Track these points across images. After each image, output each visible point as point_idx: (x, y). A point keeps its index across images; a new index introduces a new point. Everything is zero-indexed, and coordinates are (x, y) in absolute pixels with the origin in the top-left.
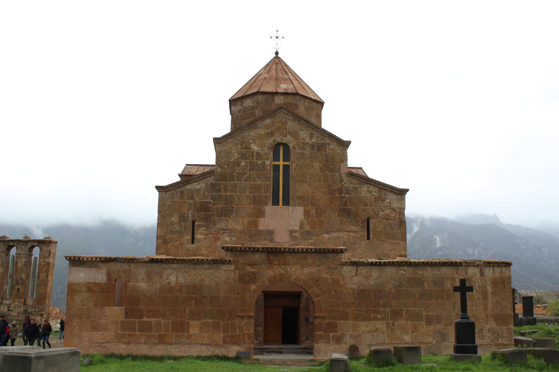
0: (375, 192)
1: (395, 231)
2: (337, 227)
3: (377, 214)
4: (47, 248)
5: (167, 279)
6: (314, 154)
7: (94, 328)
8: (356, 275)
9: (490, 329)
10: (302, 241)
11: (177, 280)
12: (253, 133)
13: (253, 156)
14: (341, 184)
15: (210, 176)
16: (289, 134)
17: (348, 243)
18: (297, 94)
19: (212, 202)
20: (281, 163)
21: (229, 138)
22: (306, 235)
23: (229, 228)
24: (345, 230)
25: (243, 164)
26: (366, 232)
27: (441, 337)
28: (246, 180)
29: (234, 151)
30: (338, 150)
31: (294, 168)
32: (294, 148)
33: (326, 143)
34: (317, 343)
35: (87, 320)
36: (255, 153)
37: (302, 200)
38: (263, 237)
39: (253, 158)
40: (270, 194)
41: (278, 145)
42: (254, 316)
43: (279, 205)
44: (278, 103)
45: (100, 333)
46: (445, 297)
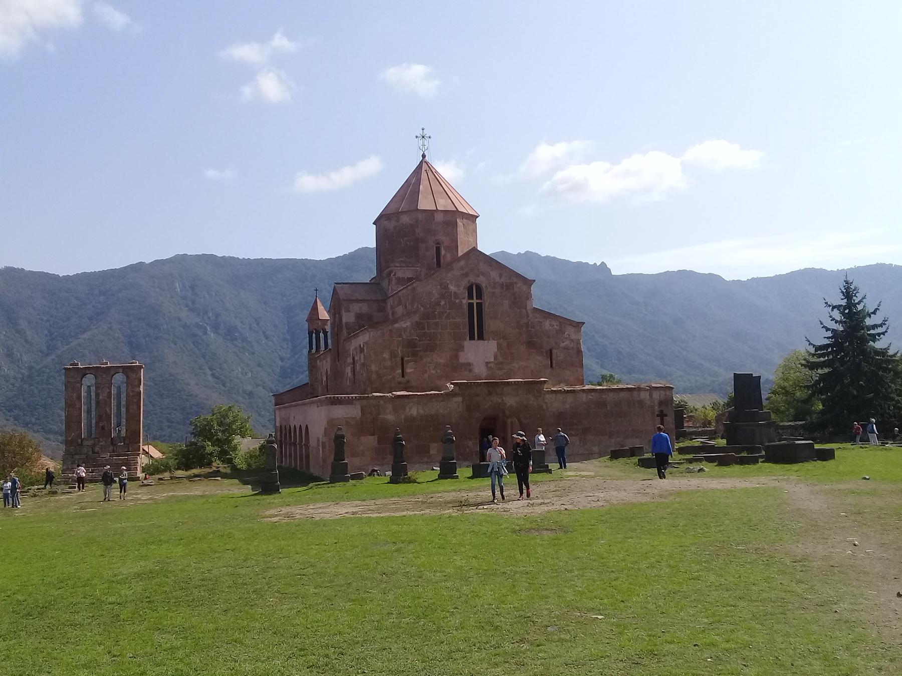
0: (557, 325)
12: (450, 275)
16: (483, 274)
19: (418, 339)
20: (475, 301)
25: (443, 303)
29: (434, 292)
30: (525, 288)
31: (487, 306)
32: (486, 287)
37: (496, 335)
38: (463, 368)
43: (474, 339)
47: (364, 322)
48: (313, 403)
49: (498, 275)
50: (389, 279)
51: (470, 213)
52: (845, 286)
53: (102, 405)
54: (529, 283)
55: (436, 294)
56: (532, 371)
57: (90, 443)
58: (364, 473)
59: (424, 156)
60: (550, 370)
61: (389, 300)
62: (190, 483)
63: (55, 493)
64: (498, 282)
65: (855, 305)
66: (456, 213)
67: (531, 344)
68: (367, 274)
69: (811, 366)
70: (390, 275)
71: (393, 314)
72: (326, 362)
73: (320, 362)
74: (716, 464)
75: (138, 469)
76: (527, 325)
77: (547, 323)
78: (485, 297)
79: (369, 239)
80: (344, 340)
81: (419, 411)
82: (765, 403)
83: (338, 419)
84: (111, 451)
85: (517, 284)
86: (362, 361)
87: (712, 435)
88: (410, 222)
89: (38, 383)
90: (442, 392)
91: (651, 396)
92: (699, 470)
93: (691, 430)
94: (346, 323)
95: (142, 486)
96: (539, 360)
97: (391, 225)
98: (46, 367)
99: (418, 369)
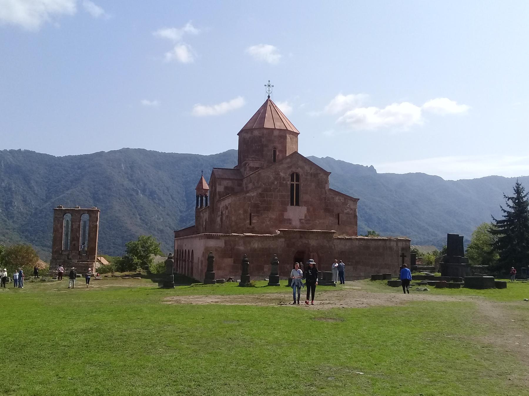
0: (343, 200)
5: (253, 245)
10: (306, 224)
12: (281, 167)
19: (260, 203)
20: (295, 183)
25: (276, 183)
29: (271, 176)
30: (324, 177)
32: (302, 175)
33: (318, 173)
37: (306, 203)
38: (286, 222)
39: (281, 181)
40: (290, 200)
43: (294, 205)
47: (229, 191)
48: (197, 237)
50: (245, 168)
51: (295, 131)
52: (516, 186)
53: (75, 231)
54: (327, 174)
55: (272, 178)
56: (327, 226)
57: (66, 253)
58: (224, 279)
59: (269, 97)
60: (338, 225)
61: (244, 180)
62: (123, 279)
63: (44, 281)
64: (309, 173)
65: (522, 198)
66: (287, 131)
67: (327, 210)
68: (232, 164)
69: (494, 232)
70: (246, 165)
71: (246, 188)
72: (206, 214)
73: (202, 214)
74: (434, 287)
75: (94, 270)
76: (325, 199)
77: (337, 198)
78: (301, 181)
79: (234, 145)
80: (217, 202)
82: (465, 253)
83: (211, 247)
84: (78, 258)
85: (320, 174)
86: (227, 214)
87: (433, 270)
88: (259, 135)
89: (40, 218)
90: (273, 235)
91: (397, 245)
92: (424, 290)
93: (420, 266)
94: (219, 192)
95: (95, 280)
96: (330, 220)
97: (247, 136)
98: (45, 208)
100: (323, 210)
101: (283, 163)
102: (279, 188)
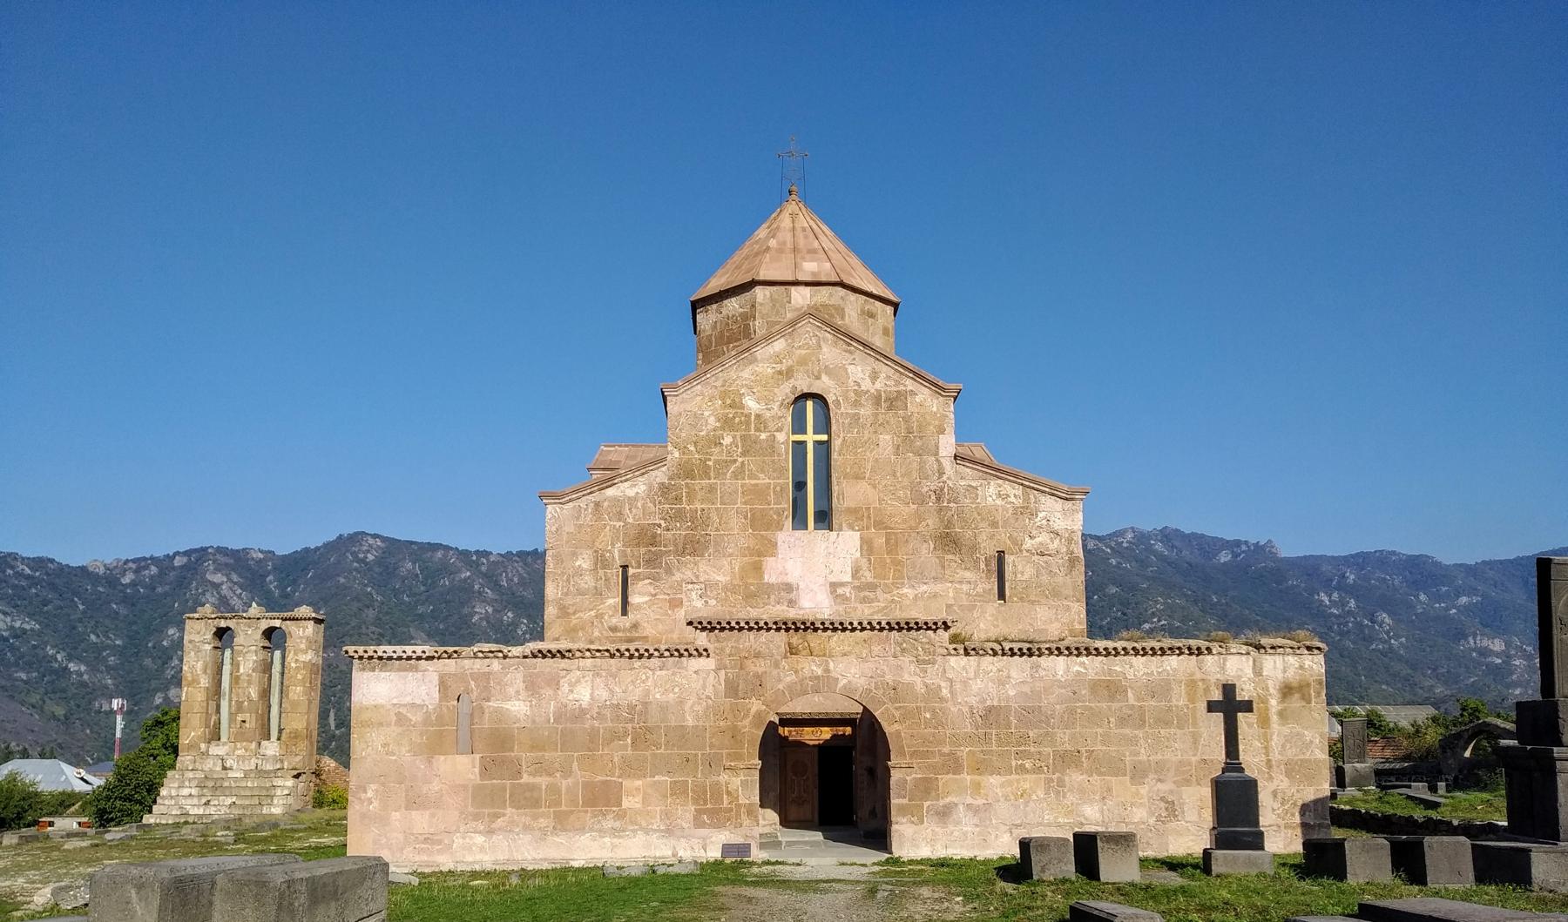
0: (1015, 495)
1: (1060, 580)
2: (933, 574)
3: (1020, 543)
4: (304, 631)
5: (572, 692)
6: (880, 417)
7: (413, 803)
8: (977, 674)
9: (1277, 793)
10: (859, 606)
11: (592, 695)
12: (746, 373)
13: (748, 423)
14: (941, 480)
15: (659, 468)
17: (956, 608)
18: (842, 284)
19: (663, 525)
20: (810, 438)
21: (695, 383)
22: (865, 589)
23: (702, 580)
24: (951, 579)
25: (727, 440)
26: (996, 583)
27: (1167, 809)
28: (735, 476)
29: (706, 414)
32: (837, 403)
34: (897, 823)
35: (398, 786)
36: (753, 417)
37: (858, 516)
38: (773, 597)
40: (787, 505)
41: (806, 396)
42: (759, 767)
44: (798, 306)
45: (428, 812)
46: (1175, 722)
49: (867, 375)
60: (996, 605)
64: (868, 391)
67: (948, 541)
78: (834, 428)
81: (596, 692)
99: (661, 597)
100: (932, 546)
101: (756, 360)
102: (740, 460)
